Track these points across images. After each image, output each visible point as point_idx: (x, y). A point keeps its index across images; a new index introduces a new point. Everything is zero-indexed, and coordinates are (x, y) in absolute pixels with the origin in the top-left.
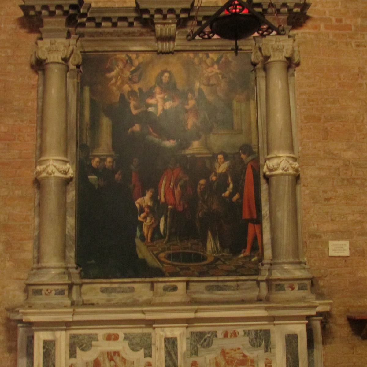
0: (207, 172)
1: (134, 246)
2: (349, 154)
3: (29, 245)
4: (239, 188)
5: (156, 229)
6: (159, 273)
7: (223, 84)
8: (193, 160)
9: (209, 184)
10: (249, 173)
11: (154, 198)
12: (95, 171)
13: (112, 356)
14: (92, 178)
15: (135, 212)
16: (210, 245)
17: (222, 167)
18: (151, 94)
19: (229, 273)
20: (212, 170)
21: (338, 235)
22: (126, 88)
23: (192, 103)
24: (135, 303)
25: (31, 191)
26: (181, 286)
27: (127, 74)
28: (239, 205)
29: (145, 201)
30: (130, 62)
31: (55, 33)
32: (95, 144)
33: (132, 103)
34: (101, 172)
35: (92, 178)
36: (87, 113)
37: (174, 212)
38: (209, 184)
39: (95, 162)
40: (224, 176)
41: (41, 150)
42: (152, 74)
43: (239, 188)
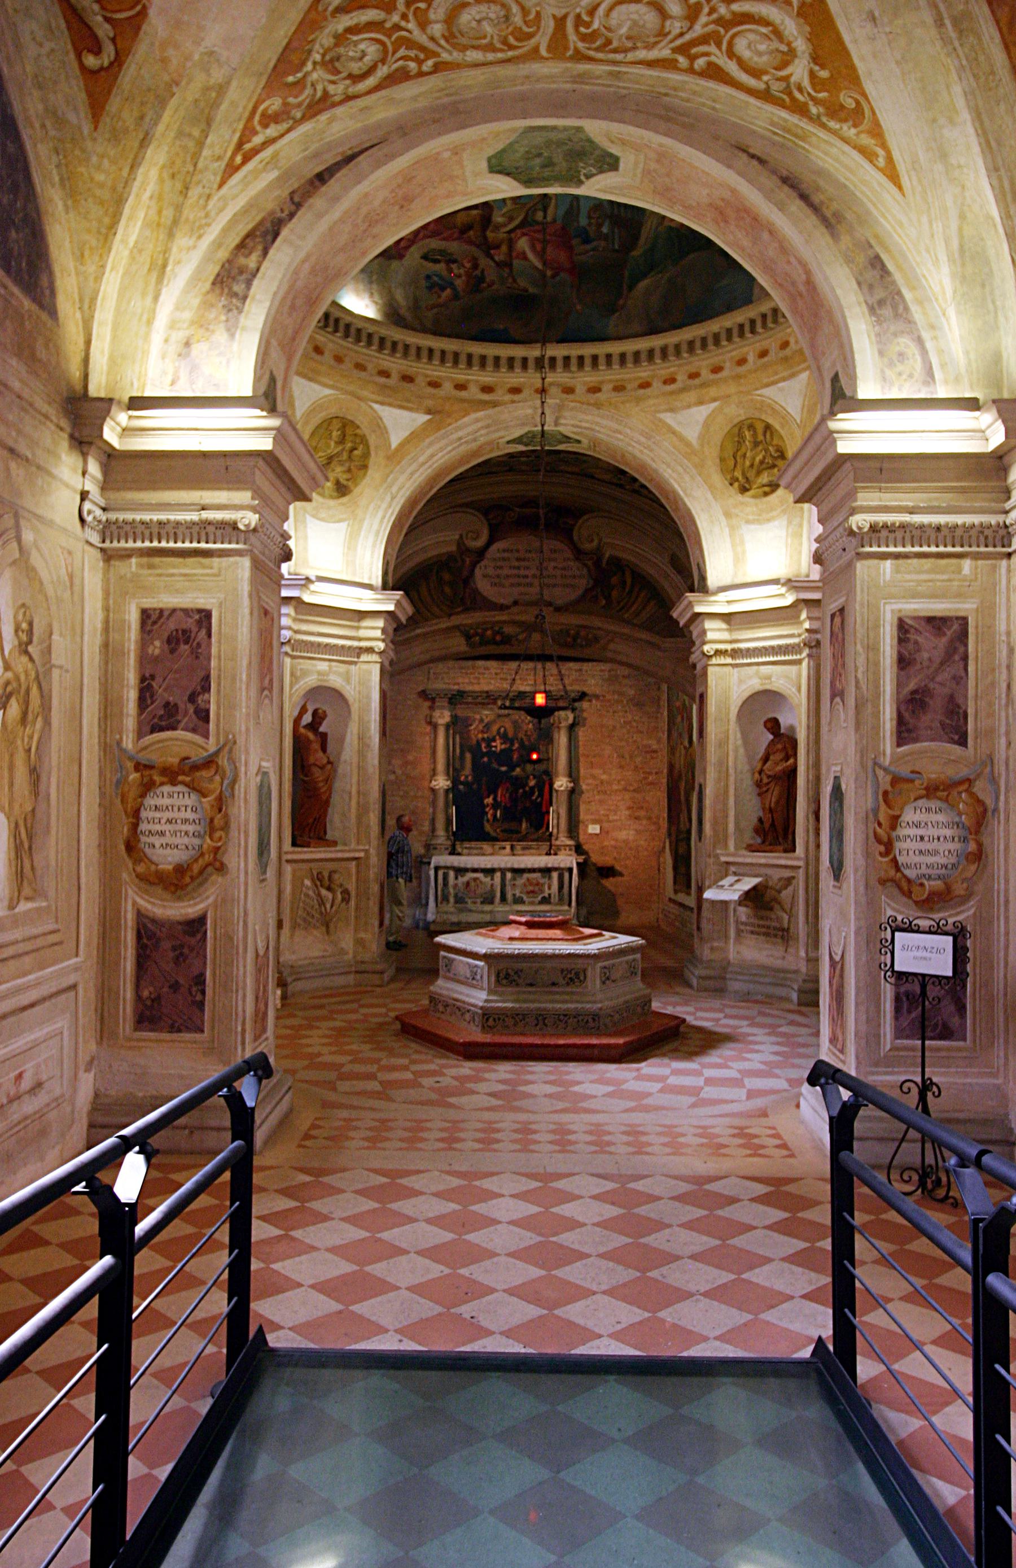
0: (524, 785)
1: (482, 826)
2: (604, 777)
3: (427, 823)
4: (541, 795)
5: (494, 815)
6: (495, 839)
7: (535, 736)
8: (517, 778)
9: (525, 792)
10: (547, 787)
11: (495, 799)
12: (462, 783)
13: (475, 879)
14: (461, 787)
15: (484, 806)
16: (524, 825)
17: (532, 783)
18: (494, 740)
19: (533, 841)
20: (527, 784)
21: (595, 822)
22: (480, 736)
23: (516, 745)
24: (484, 855)
25: (427, 793)
26: (508, 847)
27: (481, 727)
28: (541, 803)
29: (489, 800)
30: (481, 720)
31: (443, 708)
32: (463, 767)
33: (483, 745)
34: (466, 784)
35: (461, 787)
36: (458, 751)
37: (505, 807)
38: (525, 792)
39: (462, 778)
40: (532, 788)
41: (434, 773)
42: (495, 728)
43: (541, 795)
